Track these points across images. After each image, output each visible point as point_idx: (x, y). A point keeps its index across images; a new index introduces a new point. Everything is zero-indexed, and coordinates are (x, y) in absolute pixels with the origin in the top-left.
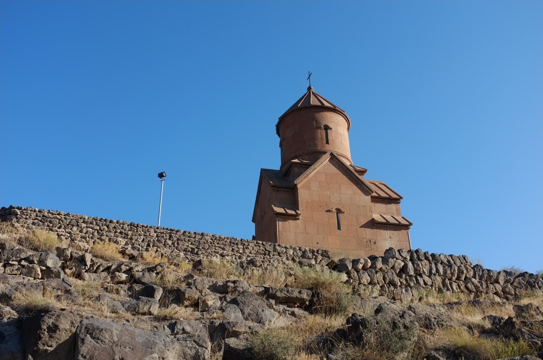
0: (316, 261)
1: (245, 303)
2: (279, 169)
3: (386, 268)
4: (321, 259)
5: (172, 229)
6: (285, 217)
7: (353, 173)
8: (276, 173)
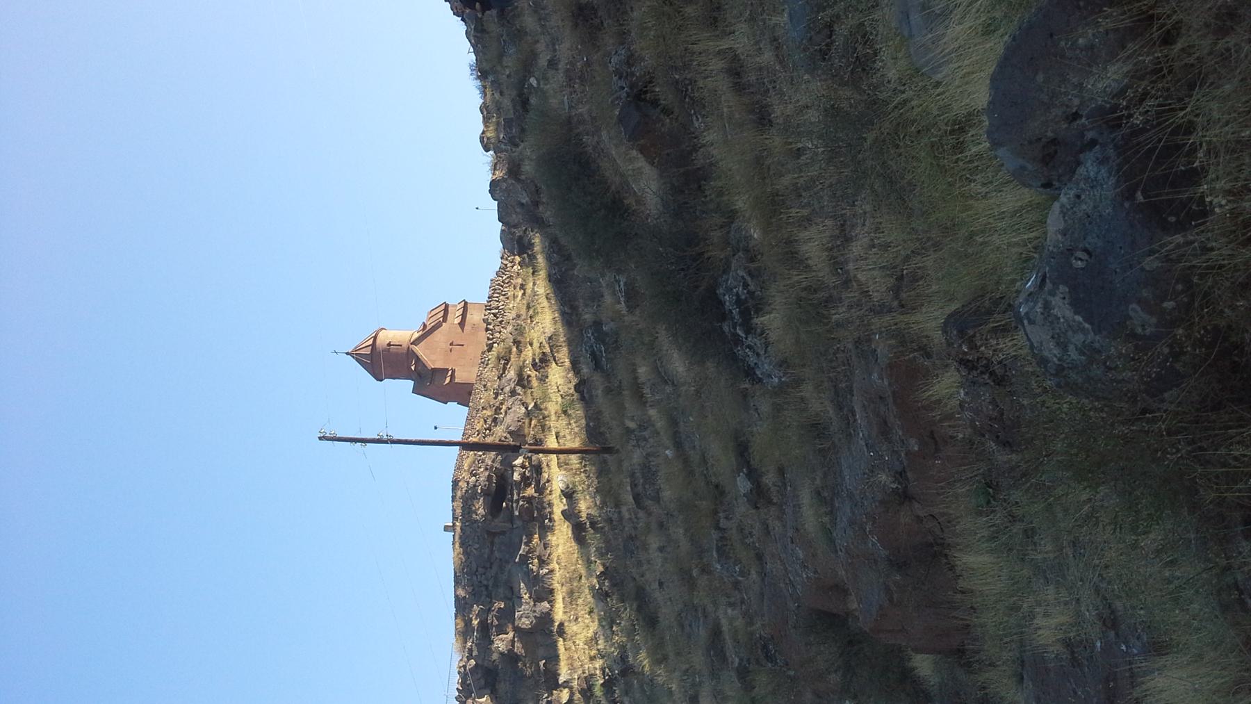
6: (453, 376)
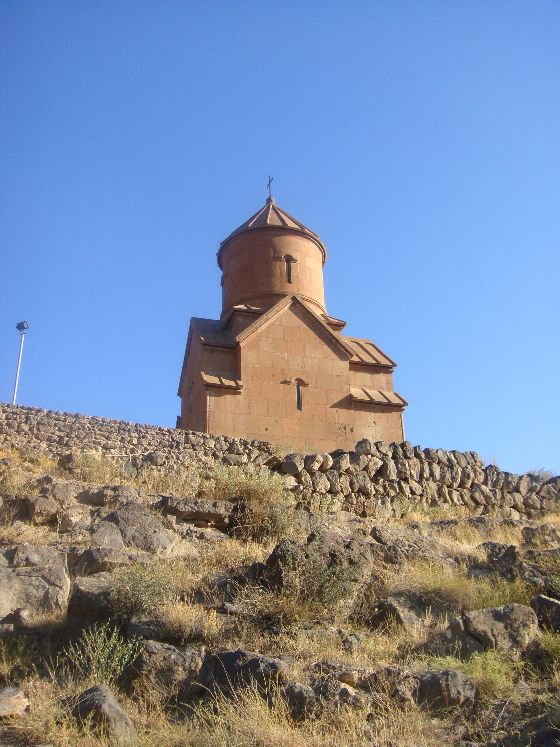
0: (249, 457)
1: (128, 521)
2: (219, 319)
3: (355, 469)
4: (257, 455)
5: (30, 407)
6: (220, 390)
7: (324, 326)
8: (213, 325)
